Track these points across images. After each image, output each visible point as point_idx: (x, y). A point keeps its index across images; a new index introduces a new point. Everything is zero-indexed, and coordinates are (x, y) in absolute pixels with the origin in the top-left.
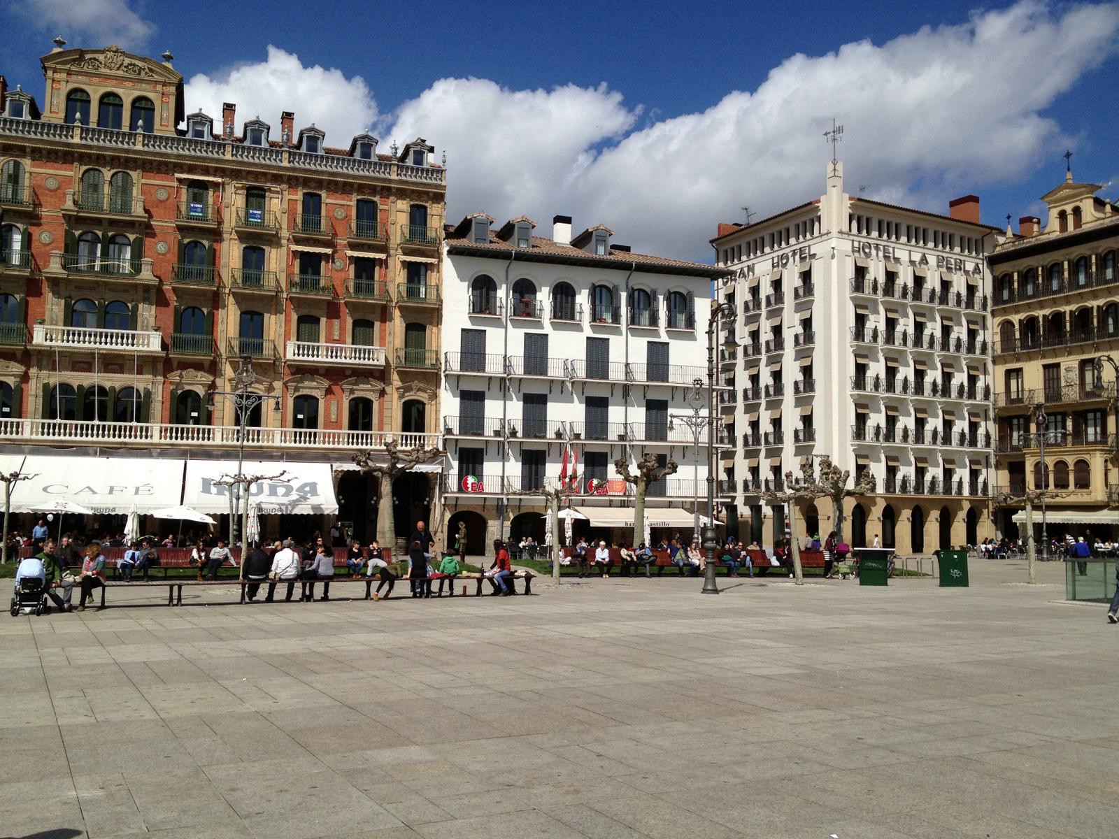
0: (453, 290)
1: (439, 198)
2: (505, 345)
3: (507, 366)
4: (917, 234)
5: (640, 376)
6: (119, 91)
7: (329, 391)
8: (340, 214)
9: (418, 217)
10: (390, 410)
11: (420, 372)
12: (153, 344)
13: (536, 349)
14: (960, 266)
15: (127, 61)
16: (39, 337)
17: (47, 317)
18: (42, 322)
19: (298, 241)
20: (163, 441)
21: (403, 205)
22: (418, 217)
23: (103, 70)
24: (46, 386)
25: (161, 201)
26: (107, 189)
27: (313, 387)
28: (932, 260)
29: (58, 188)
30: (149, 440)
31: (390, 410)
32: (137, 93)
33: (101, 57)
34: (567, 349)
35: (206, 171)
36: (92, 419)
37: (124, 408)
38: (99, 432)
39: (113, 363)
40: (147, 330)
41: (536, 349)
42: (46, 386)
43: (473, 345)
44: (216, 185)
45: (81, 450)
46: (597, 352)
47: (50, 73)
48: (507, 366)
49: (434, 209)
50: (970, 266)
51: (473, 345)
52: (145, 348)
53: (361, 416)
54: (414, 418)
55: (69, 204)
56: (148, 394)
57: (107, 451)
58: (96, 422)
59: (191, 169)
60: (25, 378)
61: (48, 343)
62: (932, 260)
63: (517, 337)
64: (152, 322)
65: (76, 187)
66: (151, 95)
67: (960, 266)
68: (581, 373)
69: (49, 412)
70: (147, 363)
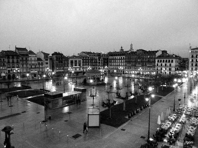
2: (159, 64)
13: (161, 64)
41: (161, 64)
43: (157, 64)
51: (157, 64)
68: (164, 66)
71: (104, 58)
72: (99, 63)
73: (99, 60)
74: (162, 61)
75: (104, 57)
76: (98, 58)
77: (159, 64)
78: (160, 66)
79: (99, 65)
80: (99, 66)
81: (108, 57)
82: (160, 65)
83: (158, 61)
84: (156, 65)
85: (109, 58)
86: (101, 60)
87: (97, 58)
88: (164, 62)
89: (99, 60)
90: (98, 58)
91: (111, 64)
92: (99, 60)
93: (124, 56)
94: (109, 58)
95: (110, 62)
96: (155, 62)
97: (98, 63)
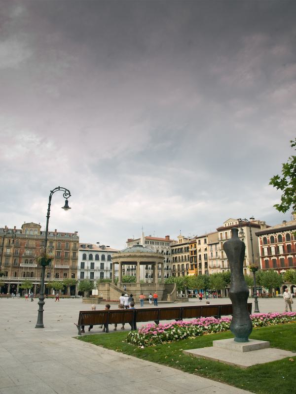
0: (80, 255)
1: (78, 242)
2: (88, 264)
3: (88, 267)
4: (157, 243)
5: (109, 268)
7: (61, 272)
8: (63, 245)
9: (75, 244)
10: (70, 275)
11: (74, 269)
12: (36, 266)
13: (92, 264)
14: (165, 248)
16: (21, 265)
19: (57, 250)
21: (72, 243)
22: (75, 244)
27: (59, 272)
28: (160, 247)
31: (70, 275)
34: (97, 264)
39: (31, 268)
41: (92, 264)
46: (102, 265)
48: (88, 267)
49: (77, 244)
50: (167, 248)
51: (83, 264)
53: (65, 275)
54: (74, 276)
62: (160, 247)
63: (90, 262)
67: (165, 248)
68: (99, 268)
70: (36, 268)
74: (94, 257)
77: (88, 264)
78: (90, 268)
82: (90, 265)
83: (84, 257)
84: (79, 265)
88: (97, 258)
96: (75, 259)
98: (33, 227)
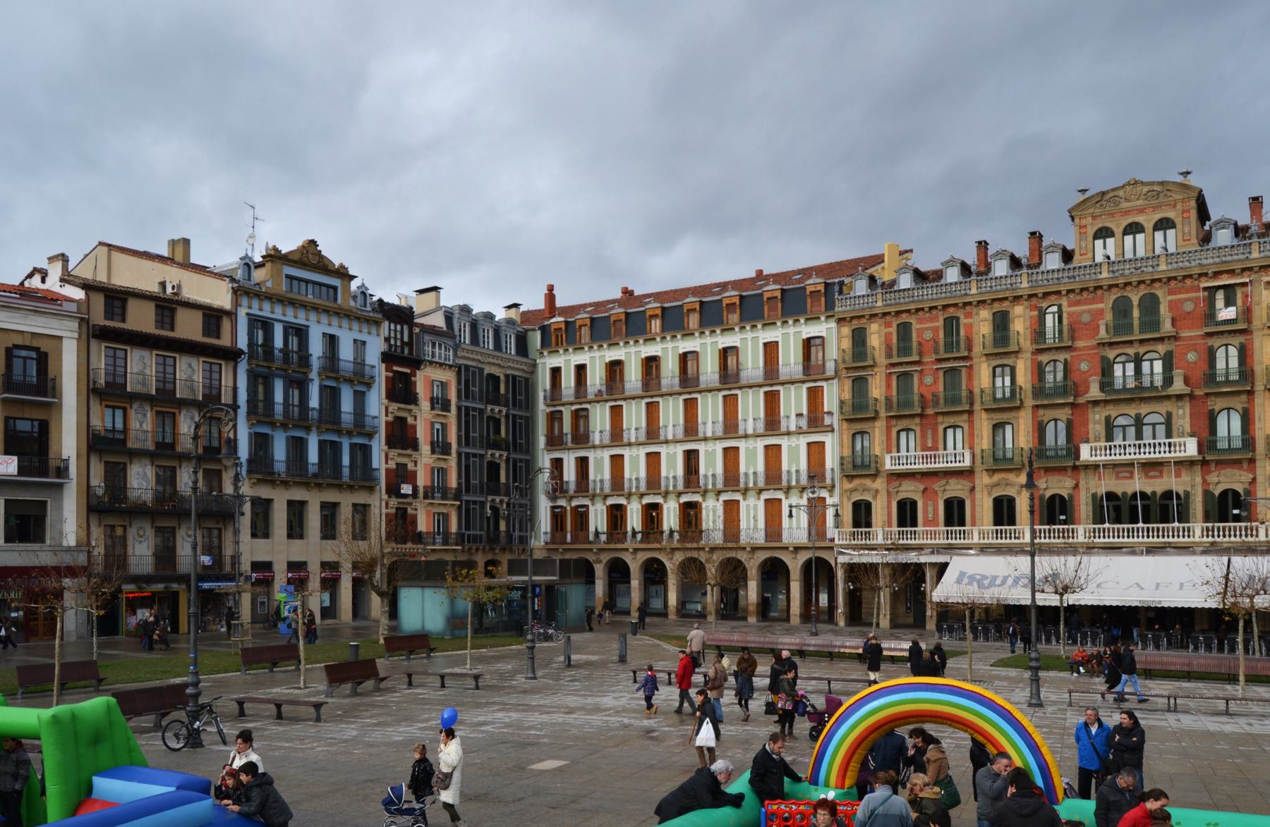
6: (1140, 219)
15: (1145, 189)
16: (1085, 453)
17: (1091, 436)
18: (1087, 442)
20: (1205, 539)
23: (1125, 205)
24: (1094, 496)
25: (1189, 313)
26: (1136, 313)
29: (1093, 321)
30: (1191, 539)
32: (1157, 217)
33: (1121, 193)
35: (1232, 272)
36: (1137, 522)
37: (1163, 509)
38: (1140, 533)
40: (1183, 436)
42: (1094, 496)
44: (1244, 285)
45: (1132, 551)
47: (1077, 220)
52: (1183, 454)
55: (1103, 332)
56: (1187, 494)
57: (1152, 550)
58: (1141, 525)
59: (1217, 274)
60: (1077, 486)
61: (1094, 458)
64: (1188, 428)
65: (1109, 316)
66: (1171, 214)
69: (1098, 518)
71: (466, 375)
72: (401, 436)
73: (401, 391)
75: (469, 357)
76: (387, 358)
79: (401, 475)
80: (393, 490)
81: (516, 367)
85: (544, 381)
86: (423, 380)
87: (373, 355)
89: (401, 391)
90: (375, 348)
91: (570, 474)
92: (392, 395)
93: (822, 328)
94: (544, 381)
95: (554, 441)
97: (378, 447)
98: (1141, 211)
